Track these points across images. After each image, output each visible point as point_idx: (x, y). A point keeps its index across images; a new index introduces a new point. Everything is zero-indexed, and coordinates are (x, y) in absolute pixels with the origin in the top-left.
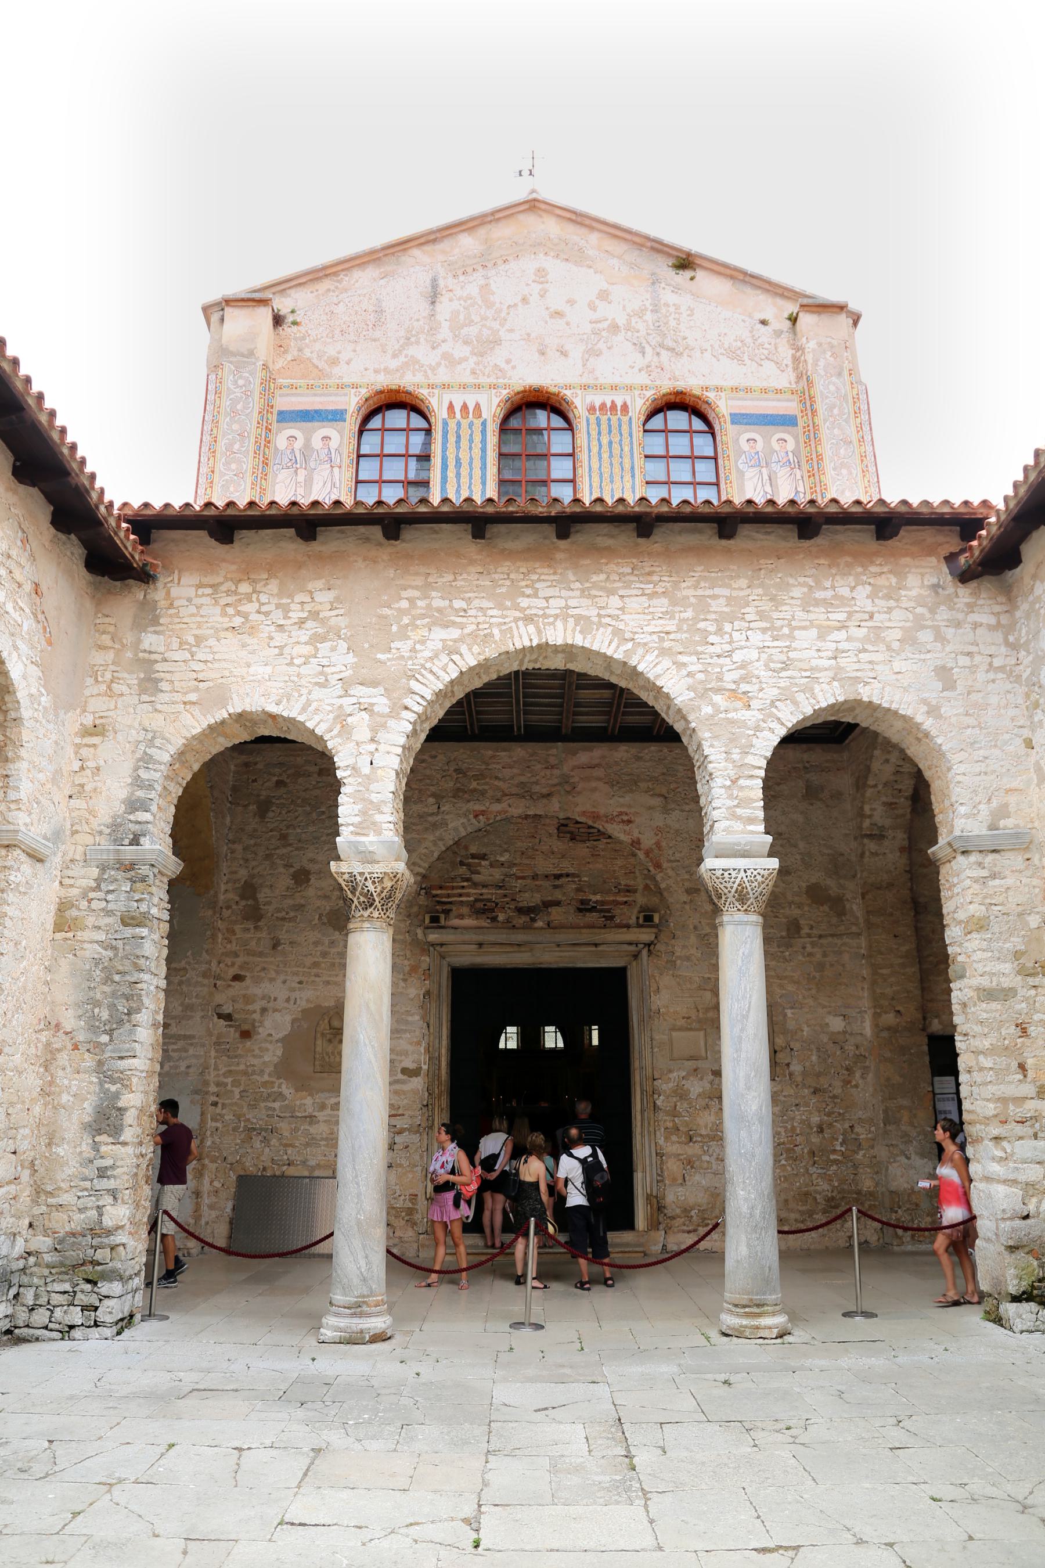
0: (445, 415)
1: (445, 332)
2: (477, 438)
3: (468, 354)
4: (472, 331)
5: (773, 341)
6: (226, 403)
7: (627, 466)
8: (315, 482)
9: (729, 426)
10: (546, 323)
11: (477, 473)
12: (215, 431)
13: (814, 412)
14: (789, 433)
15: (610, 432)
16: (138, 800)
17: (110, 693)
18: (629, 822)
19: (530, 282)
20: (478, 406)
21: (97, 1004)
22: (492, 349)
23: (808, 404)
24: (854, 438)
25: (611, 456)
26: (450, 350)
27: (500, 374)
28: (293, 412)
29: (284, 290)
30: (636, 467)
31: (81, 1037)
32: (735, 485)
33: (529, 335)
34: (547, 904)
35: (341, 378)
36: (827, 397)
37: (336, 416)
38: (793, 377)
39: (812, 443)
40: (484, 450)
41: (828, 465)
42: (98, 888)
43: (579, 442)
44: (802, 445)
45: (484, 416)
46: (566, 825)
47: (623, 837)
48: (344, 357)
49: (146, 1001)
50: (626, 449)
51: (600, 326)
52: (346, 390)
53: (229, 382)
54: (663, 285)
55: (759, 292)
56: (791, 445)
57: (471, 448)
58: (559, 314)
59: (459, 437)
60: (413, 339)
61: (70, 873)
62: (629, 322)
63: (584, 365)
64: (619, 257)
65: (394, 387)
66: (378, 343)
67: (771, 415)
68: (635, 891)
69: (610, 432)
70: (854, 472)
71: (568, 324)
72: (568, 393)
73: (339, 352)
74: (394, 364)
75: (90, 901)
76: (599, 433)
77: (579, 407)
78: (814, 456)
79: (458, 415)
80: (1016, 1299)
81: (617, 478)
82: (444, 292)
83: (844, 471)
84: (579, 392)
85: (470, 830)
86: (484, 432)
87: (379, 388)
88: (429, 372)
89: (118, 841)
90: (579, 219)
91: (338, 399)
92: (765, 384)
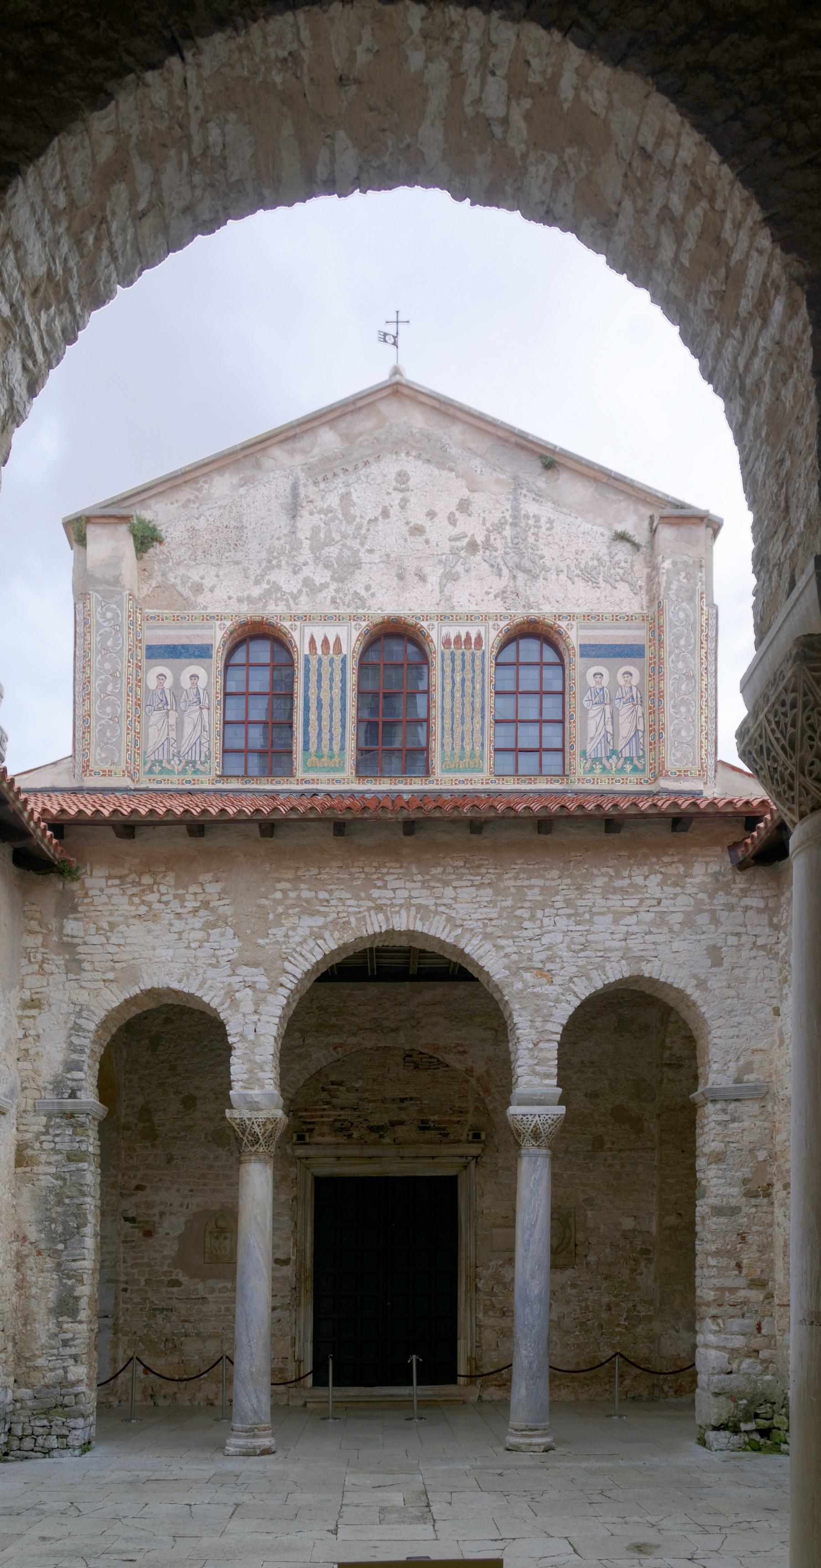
0: (307, 652)
1: (306, 554)
2: (337, 677)
3: (328, 580)
4: (333, 551)
5: (629, 559)
6: (95, 639)
7: (478, 706)
8: (186, 725)
10: (406, 540)
11: (337, 715)
12: (87, 670)
13: (661, 643)
14: (635, 665)
16: (73, 1061)
17: (42, 972)
18: (464, 1052)
19: (391, 490)
20: (338, 640)
21: (52, 1220)
22: (352, 573)
23: (657, 634)
25: (463, 696)
26: (311, 575)
27: (359, 603)
28: (160, 647)
29: (144, 500)
31: (42, 1246)
32: (578, 725)
33: (388, 556)
34: (393, 1124)
35: (205, 608)
36: (676, 626)
37: (202, 652)
38: (645, 602)
39: (656, 676)
40: (343, 690)
41: (668, 703)
42: (46, 1133)
44: (647, 678)
45: (344, 651)
46: (410, 1056)
47: (458, 1066)
48: (207, 583)
49: (90, 1217)
50: (478, 687)
51: (459, 544)
52: (211, 622)
53: (96, 617)
54: (524, 491)
55: (621, 497)
56: (635, 680)
57: (331, 688)
58: (417, 530)
59: (320, 676)
60: (274, 562)
61: (24, 1121)
62: (488, 538)
63: (441, 592)
64: (482, 457)
65: (257, 619)
66: (240, 567)
68: (467, 1112)
70: (693, 709)
71: (427, 542)
72: (425, 624)
73: (202, 578)
74: (256, 592)
75: (41, 1143)
76: (453, 670)
77: (435, 641)
78: (656, 692)
79: (319, 651)
80: (716, 1428)
81: (468, 719)
82: (304, 504)
83: (683, 709)
84: (435, 623)
85: (330, 1060)
86: (343, 670)
87: (243, 619)
88: (291, 601)
89: (60, 1094)
90: (443, 408)
91: (204, 632)
92: (616, 610)
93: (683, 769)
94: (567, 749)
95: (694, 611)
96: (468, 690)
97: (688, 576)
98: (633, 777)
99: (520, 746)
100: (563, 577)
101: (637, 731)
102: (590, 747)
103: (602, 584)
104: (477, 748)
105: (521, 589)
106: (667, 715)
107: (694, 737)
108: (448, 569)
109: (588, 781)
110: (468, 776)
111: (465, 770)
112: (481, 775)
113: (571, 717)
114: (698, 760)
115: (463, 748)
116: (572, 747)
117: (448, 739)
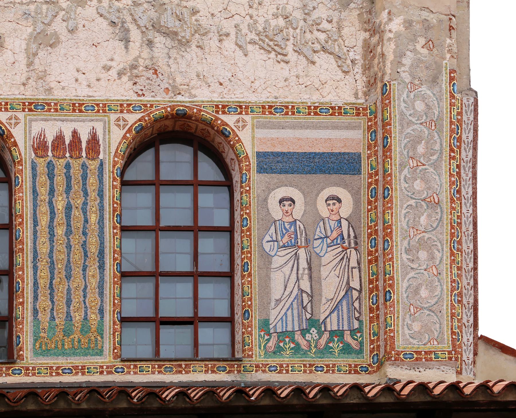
7: (93, 249)
9: (255, 177)
13: (387, 149)
14: (345, 186)
15: (69, 188)
23: (380, 136)
24: (445, 198)
25: (69, 232)
30: (107, 251)
32: (256, 281)
36: (410, 123)
38: (361, 85)
39: (380, 204)
43: (18, 207)
44: (364, 206)
50: (93, 218)
63: (30, 64)
67: (321, 155)
69: (69, 188)
70: (438, 255)
76: (52, 192)
78: (380, 227)
81: (77, 271)
83: (423, 255)
84: (21, 115)
92: (315, 98)
93: (422, 348)
94: (238, 318)
95: (439, 100)
96: (77, 223)
97: (430, 45)
98: (344, 361)
99: (163, 313)
100: (229, 44)
101: (349, 289)
102: (274, 315)
103: (292, 57)
104: (93, 317)
105: (162, 64)
106: (398, 264)
107: (440, 299)
108: (40, 27)
109: (272, 369)
110: (78, 361)
111: (74, 352)
112: (99, 360)
113: (245, 267)
114: (447, 335)
115: (69, 317)
116: (246, 314)
117: (44, 302)
